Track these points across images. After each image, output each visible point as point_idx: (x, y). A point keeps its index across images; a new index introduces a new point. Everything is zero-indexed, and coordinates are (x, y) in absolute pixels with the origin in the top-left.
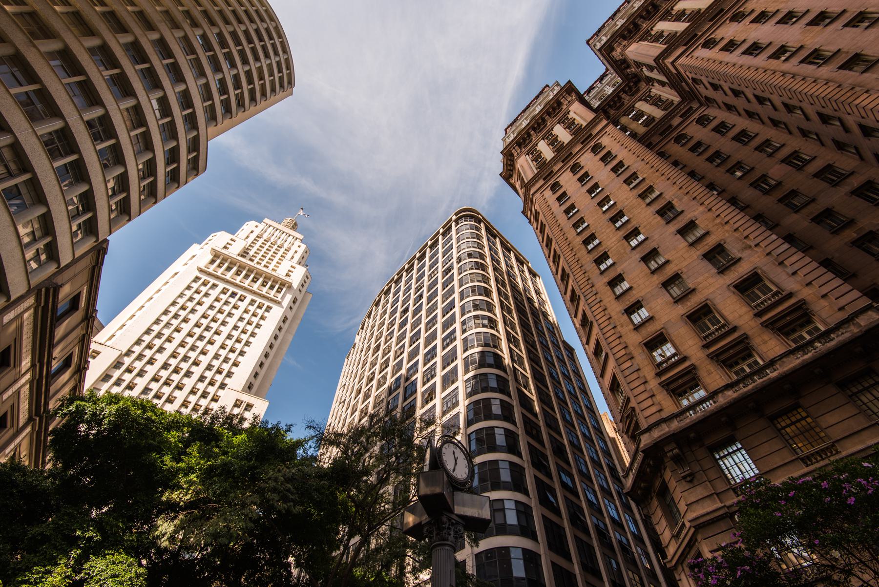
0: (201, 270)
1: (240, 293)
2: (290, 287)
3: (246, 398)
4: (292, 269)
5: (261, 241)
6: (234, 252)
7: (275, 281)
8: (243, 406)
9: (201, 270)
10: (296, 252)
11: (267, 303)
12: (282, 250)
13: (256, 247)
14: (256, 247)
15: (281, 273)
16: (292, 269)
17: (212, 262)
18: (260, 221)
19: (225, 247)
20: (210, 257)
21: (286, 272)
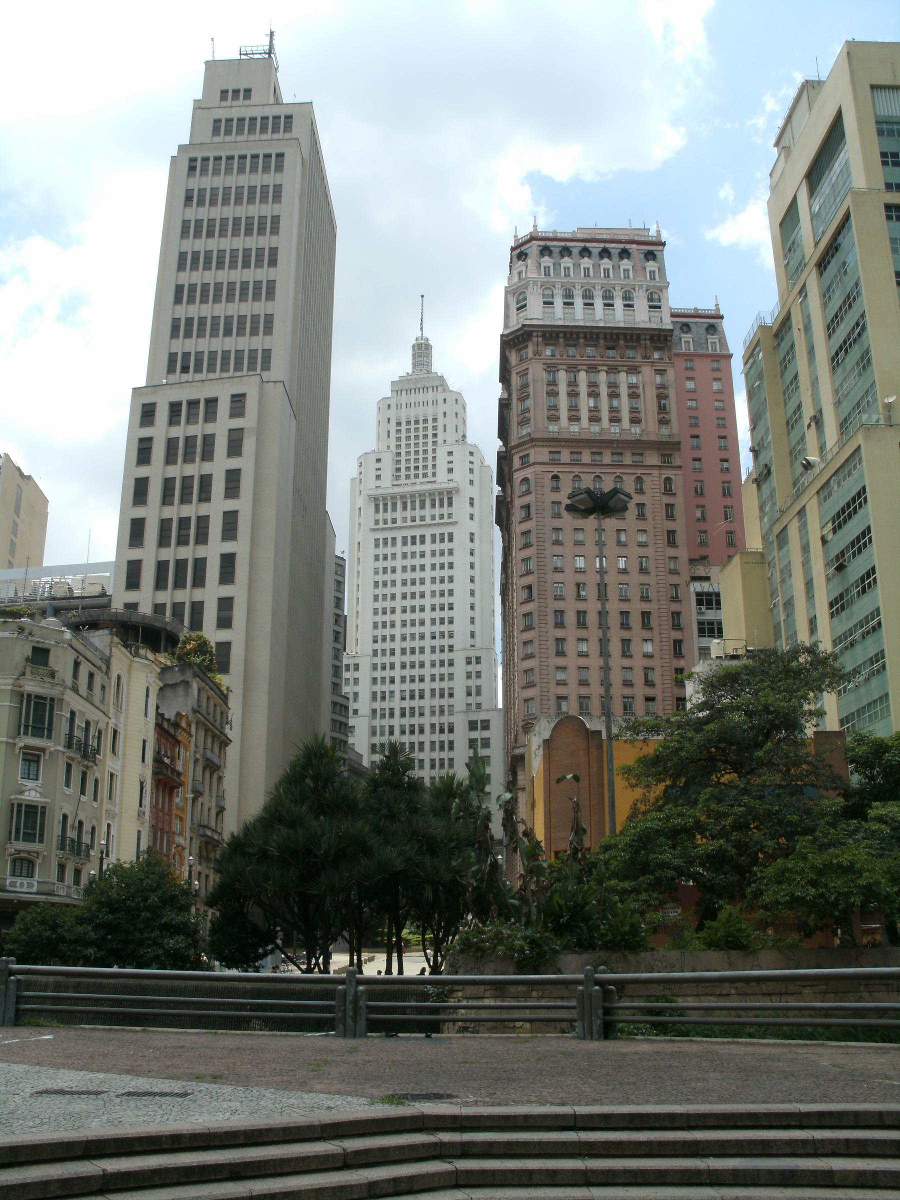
0: (375, 530)
2: (457, 490)
3: (472, 654)
4: (450, 458)
5: (404, 427)
6: (387, 485)
8: (474, 661)
9: (375, 530)
10: (445, 413)
12: (430, 424)
13: (403, 442)
14: (403, 442)
15: (442, 480)
16: (450, 458)
19: (378, 477)
20: (373, 505)
21: (446, 466)
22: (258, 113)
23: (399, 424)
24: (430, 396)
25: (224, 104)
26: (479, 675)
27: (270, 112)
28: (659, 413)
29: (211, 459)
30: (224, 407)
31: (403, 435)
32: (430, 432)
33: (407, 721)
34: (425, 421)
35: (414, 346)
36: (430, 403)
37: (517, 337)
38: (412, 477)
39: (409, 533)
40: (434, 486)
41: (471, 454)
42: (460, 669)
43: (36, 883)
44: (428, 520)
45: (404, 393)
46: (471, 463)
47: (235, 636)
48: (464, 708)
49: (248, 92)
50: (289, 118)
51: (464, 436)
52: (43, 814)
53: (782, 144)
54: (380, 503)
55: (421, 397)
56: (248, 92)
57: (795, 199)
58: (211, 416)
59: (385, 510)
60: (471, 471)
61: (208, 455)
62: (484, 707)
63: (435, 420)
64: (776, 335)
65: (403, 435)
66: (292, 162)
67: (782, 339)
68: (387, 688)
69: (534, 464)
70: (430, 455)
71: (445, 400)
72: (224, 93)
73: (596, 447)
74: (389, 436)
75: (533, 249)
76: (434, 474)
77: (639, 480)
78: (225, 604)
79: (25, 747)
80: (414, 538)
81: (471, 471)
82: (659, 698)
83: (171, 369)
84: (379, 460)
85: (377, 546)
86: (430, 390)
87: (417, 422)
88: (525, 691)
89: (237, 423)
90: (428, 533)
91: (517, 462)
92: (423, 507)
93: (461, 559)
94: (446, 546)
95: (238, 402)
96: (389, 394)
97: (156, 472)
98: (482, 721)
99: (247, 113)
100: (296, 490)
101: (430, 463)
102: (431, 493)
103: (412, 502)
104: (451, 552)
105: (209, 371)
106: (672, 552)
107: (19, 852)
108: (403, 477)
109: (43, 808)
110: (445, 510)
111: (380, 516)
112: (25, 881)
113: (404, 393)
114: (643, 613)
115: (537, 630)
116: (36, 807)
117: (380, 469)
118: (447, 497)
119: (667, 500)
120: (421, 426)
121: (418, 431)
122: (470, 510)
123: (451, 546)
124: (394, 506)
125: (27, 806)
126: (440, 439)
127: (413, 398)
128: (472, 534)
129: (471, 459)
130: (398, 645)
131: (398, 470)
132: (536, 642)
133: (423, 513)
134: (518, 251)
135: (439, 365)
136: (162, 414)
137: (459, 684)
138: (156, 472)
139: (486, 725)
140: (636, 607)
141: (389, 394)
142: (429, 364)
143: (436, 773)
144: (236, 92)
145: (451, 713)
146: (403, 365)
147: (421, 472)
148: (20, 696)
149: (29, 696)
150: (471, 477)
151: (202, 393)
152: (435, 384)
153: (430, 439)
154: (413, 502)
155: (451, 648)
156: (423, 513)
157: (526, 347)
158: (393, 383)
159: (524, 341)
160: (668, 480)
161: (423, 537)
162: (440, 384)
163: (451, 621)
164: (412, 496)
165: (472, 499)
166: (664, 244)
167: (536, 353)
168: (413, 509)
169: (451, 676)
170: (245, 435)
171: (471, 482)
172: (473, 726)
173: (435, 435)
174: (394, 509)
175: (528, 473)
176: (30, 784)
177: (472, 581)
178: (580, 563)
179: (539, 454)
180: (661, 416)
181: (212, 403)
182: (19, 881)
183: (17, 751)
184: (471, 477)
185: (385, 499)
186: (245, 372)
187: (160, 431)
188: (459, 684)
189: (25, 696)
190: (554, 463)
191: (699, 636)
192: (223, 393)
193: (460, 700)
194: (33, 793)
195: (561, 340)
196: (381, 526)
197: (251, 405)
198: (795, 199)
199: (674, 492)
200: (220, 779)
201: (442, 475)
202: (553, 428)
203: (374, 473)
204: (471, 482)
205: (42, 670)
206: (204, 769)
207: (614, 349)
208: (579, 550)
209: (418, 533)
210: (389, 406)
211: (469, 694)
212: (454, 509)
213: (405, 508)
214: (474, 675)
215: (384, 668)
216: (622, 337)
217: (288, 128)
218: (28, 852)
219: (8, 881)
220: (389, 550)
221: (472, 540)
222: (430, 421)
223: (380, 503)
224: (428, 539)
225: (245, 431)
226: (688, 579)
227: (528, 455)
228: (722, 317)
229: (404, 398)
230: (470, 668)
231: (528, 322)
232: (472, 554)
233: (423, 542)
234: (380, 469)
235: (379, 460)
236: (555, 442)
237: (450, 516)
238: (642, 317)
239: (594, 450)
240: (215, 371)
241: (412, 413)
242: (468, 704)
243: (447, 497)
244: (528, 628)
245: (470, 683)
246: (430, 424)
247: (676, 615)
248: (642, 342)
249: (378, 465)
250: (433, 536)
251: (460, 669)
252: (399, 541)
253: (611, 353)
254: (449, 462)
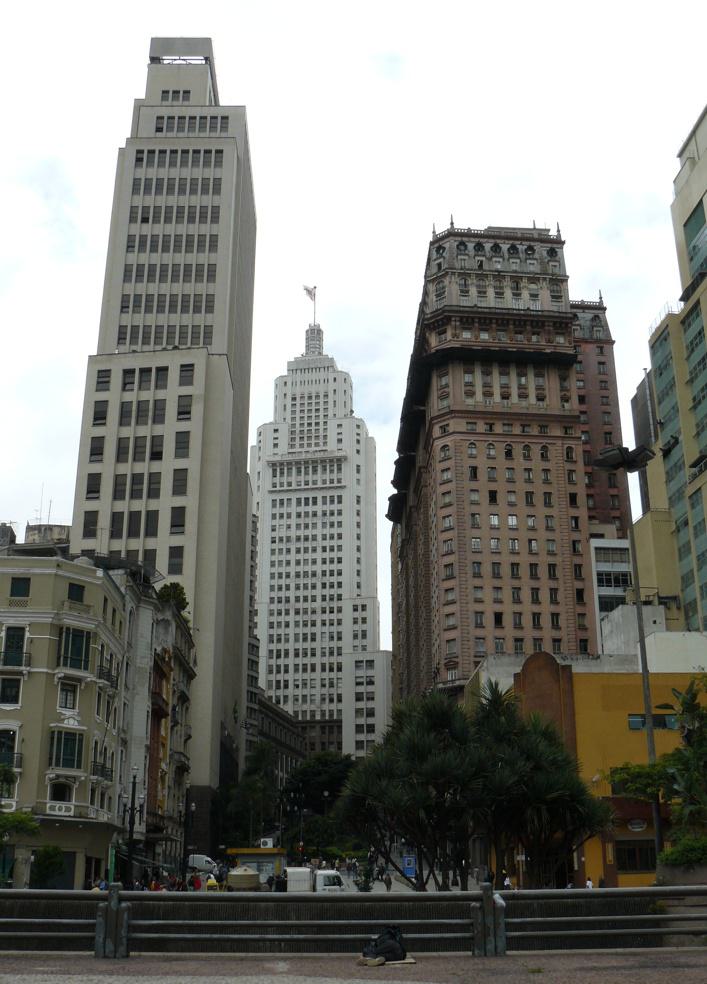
0: (271, 492)
1: (310, 495)
2: (346, 458)
3: (359, 602)
5: (298, 402)
7: (331, 461)
8: (360, 608)
9: (271, 492)
11: (336, 493)
12: (322, 400)
17: (274, 471)
19: (276, 445)
21: (336, 437)
22: (197, 112)
23: (294, 399)
24: (322, 375)
25: (164, 103)
26: (364, 620)
27: (209, 112)
28: (561, 391)
29: (162, 421)
30: (174, 375)
31: (298, 408)
32: (321, 407)
33: (300, 661)
34: (317, 397)
35: (307, 331)
36: (322, 381)
37: (437, 321)
38: (305, 445)
39: (303, 495)
40: (326, 455)
41: (358, 426)
42: (348, 615)
43: (73, 807)
44: (320, 485)
45: (299, 371)
46: (358, 434)
47: (186, 581)
48: (352, 651)
49: (187, 92)
50: (225, 118)
51: (352, 412)
52: (81, 741)
53: (687, 154)
54: (277, 467)
55: (314, 376)
56: (187, 92)
57: (701, 200)
58: (162, 383)
59: (282, 473)
60: (358, 441)
61: (159, 418)
62: (368, 649)
63: (326, 396)
64: (683, 322)
65: (298, 408)
66: (229, 158)
67: (689, 325)
68: (281, 631)
69: (454, 433)
70: (321, 427)
71: (335, 379)
72: (165, 92)
73: (508, 419)
74: (285, 409)
75: (450, 244)
76: (325, 443)
77: (544, 448)
78: (176, 553)
79: (66, 677)
80: (307, 499)
81: (358, 441)
82: (565, 639)
83: (121, 339)
84: (276, 431)
85: (274, 506)
86: (322, 370)
87: (310, 398)
88: (448, 633)
89: (185, 390)
90: (319, 495)
91: (437, 431)
92: (315, 471)
93: (348, 519)
94: (335, 507)
95: (187, 370)
96: (286, 373)
97: (111, 431)
98: (367, 661)
99: (187, 112)
100: (232, 452)
101: (321, 433)
102: (323, 461)
103: (305, 468)
104: (340, 513)
105: (143, 343)
106: (574, 512)
107: (58, 776)
108: (298, 445)
109: (81, 735)
110: (335, 476)
111: (277, 480)
112: (63, 804)
113: (299, 371)
114: (550, 565)
115: (457, 579)
116: (74, 734)
117: (276, 438)
118: (339, 462)
119: (569, 466)
120: (314, 401)
122: (356, 476)
123: (340, 507)
124: (289, 469)
125: (66, 733)
126: (330, 413)
127: (307, 376)
128: (358, 497)
129: (358, 431)
130: (292, 594)
131: (293, 439)
132: (457, 589)
133: (315, 478)
134: (436, 245)
135: (329, 348)
136: (116, 380)
137: (347, 629)
138: (111, 431)
139: (370, 663)
140: (544, 561)
141: (286, 373)
142: (321, 347)
143: (327, 707)
144: (176, 92)
145: (339, 654)
146: (298, 348)
147: (313, 441)
148: (60, 630)
149: (68, 629)
150: (358, 447)
151: (154, 362)
153: (321, 413)
155: (340, 597)
156: (315, 478)
157: (445, 332)
158: (289, 363)
159: (444, 324)
160: (570, 449)
161: (315, 499)
162: (329, 365)
163: (340, 573)
164: (306, 462)
165: (358, 466)
166: (564, 243)
167: (455, 335)
168: (307, 473)
169: (339, 622)
170: (194, 402)
171: (358, 452)
172: (358, 664)
174: (289, 474)
175: (448, 441)
176: (68, 713)
177: (358, 538)
178: (495, 521)
179: (456, 425)
180: (563, 393)
181: (163, 371)
182: (58, 804)
183: (56, 680)
184: (358, 447)
185: (282, 464)
186: (201, 345)
187: (114, 396)
188: (347, 629)
189: (64, 630)
190: (473, 433)
191: (599, 586)
192: (174, 361)
193: (347, 643)
194: (72, 721)
195: (477, 325)
196: (278, 488)
197: (199, 374)
198: (701, 200)
199: (574, 459)
200: (187, 708)
201: (332, 445)
202: (470, 401)
203: (272, 442)
204: (358, 452)
205: (78, 605)
206: (179, 699)
207: (521, 333)
208: (513, 510)
209: (310, 495)
210: (286, 383)
211: (355, 636)
212: (342, 476)
213: (299, 472)
214: (360, 621)
215: (280, 614)
216: (528, 323)
217: (224, 128)
218: (67, 777)
219: (48, 805)
220: (284, 510)
221: (358, 502)
222: (322, 396)
223: (277, 467)
224: (320, 501)
225: (194, 398)
226: (588, 536)
227: (448, 425)
228: (605, 309)
229: (299, 377)
230: (356, 614)
231: (446, 308)
232: (358, 514)
233: (315, 502)
234: (276, 438)
235: (276, 431)
236: (471, 415)
237: (339, 481)
238: (544, 303)
239: (506, 422)
240: (149, 344)
241: (307, 390)
242: (355, 646)
243: (339, 462)
244: (450, 577)
245: (356, 627)
246: (322, 400)
247: (578, 568)
248: (547, 328)
250: (324, 498)
251: (348, 615)
252: (294, 502)
253: (520, 337)
254: (339, 434)
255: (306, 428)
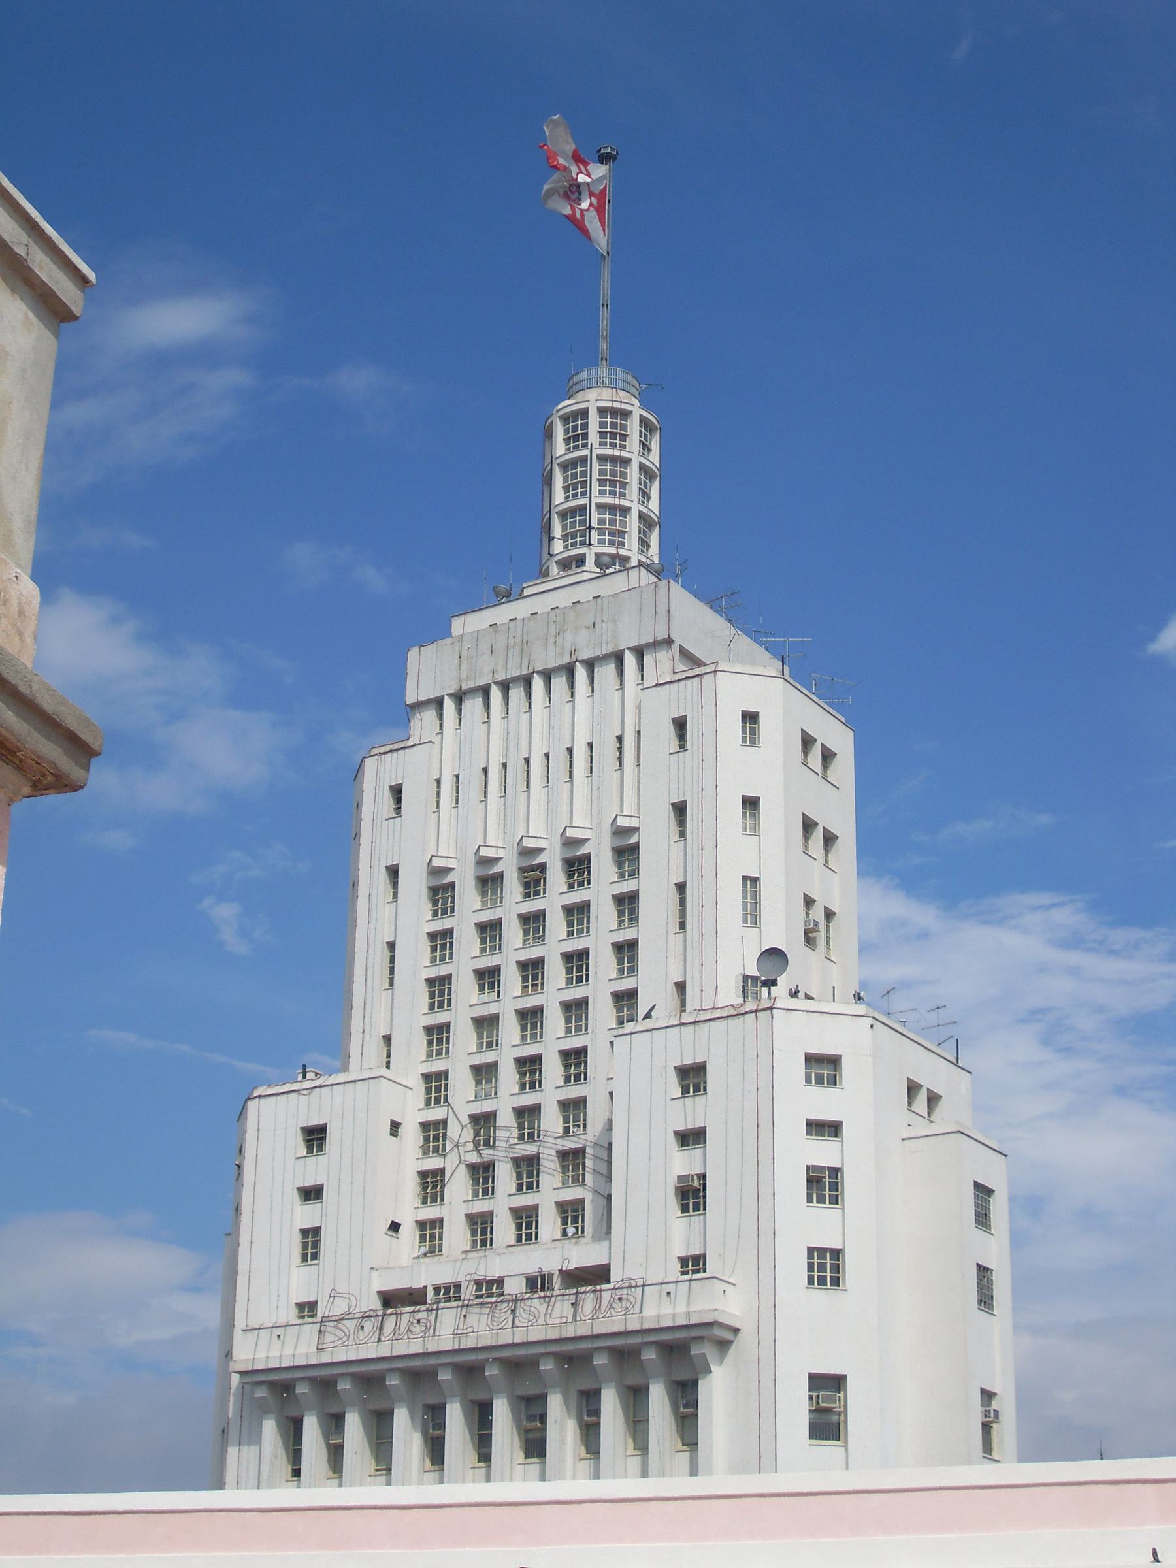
2: (719, 1335)
10: (680, 810)
16: (691, 1113)
18: (395, 715)
23: (441, 893)
34: (578, 868)
41: (824, 1067)
63: (627, 854)
71: (680, 725)
117: (312, 1194)
121: (540, 938)
129: (824, 1103)
152: (628, 639)
154: (481, 1416)
165: (827, 1385)
171: (826, 1267)
173: (627, 951)
204: (826, 1267)
249: (314, 1171)
255: (508, 1095)
